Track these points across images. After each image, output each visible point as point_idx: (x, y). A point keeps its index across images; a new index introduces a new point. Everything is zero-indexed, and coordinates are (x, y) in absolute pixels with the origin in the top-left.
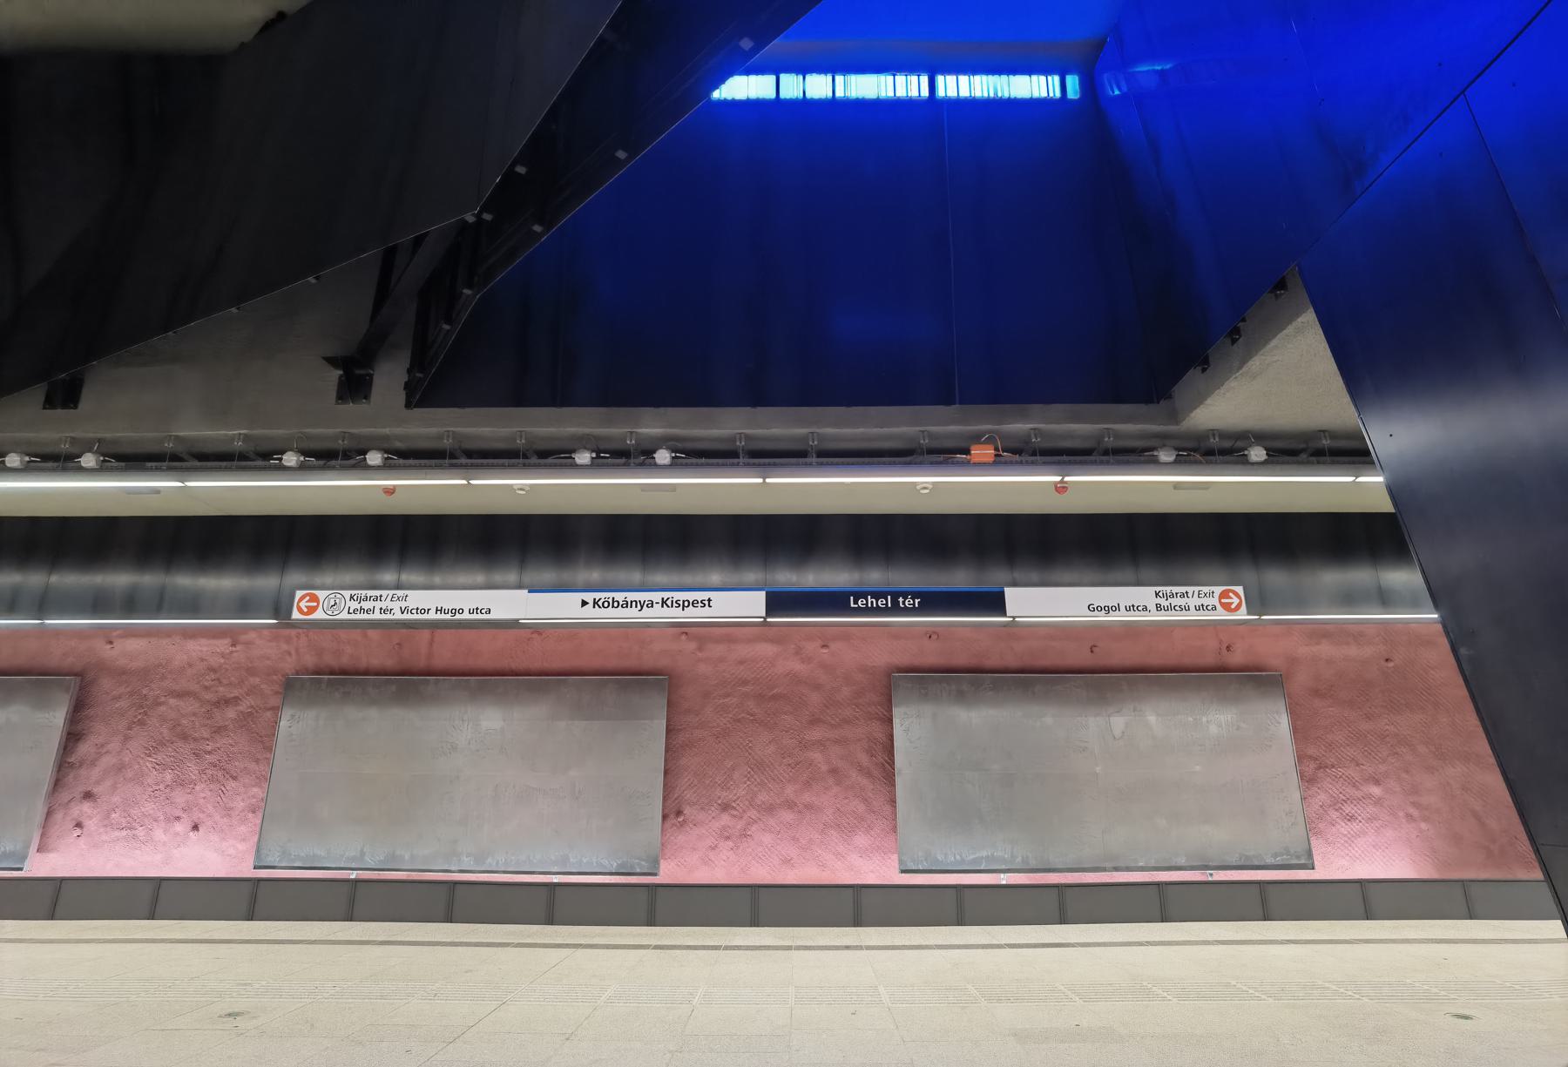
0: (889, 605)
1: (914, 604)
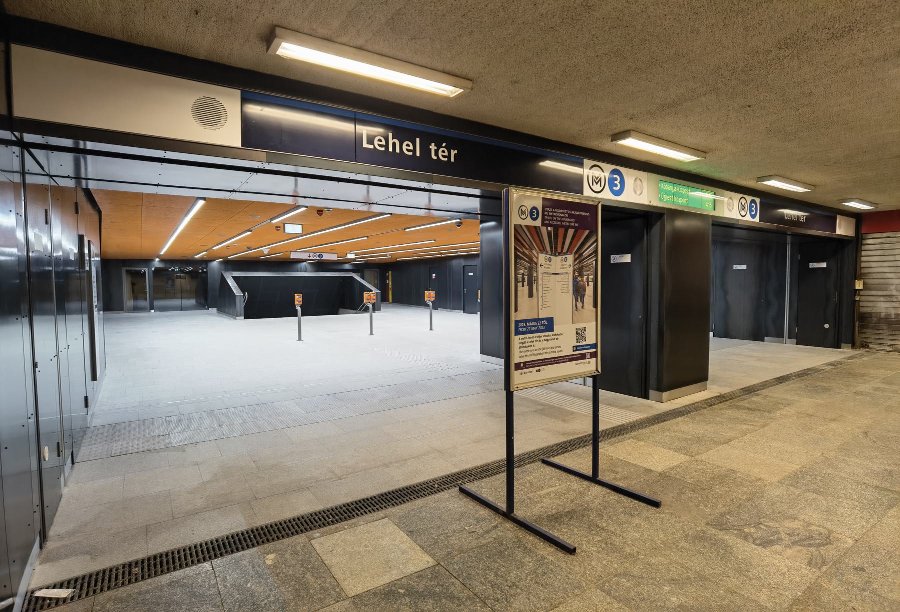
0: (418, 154)
1: (449, 157)
